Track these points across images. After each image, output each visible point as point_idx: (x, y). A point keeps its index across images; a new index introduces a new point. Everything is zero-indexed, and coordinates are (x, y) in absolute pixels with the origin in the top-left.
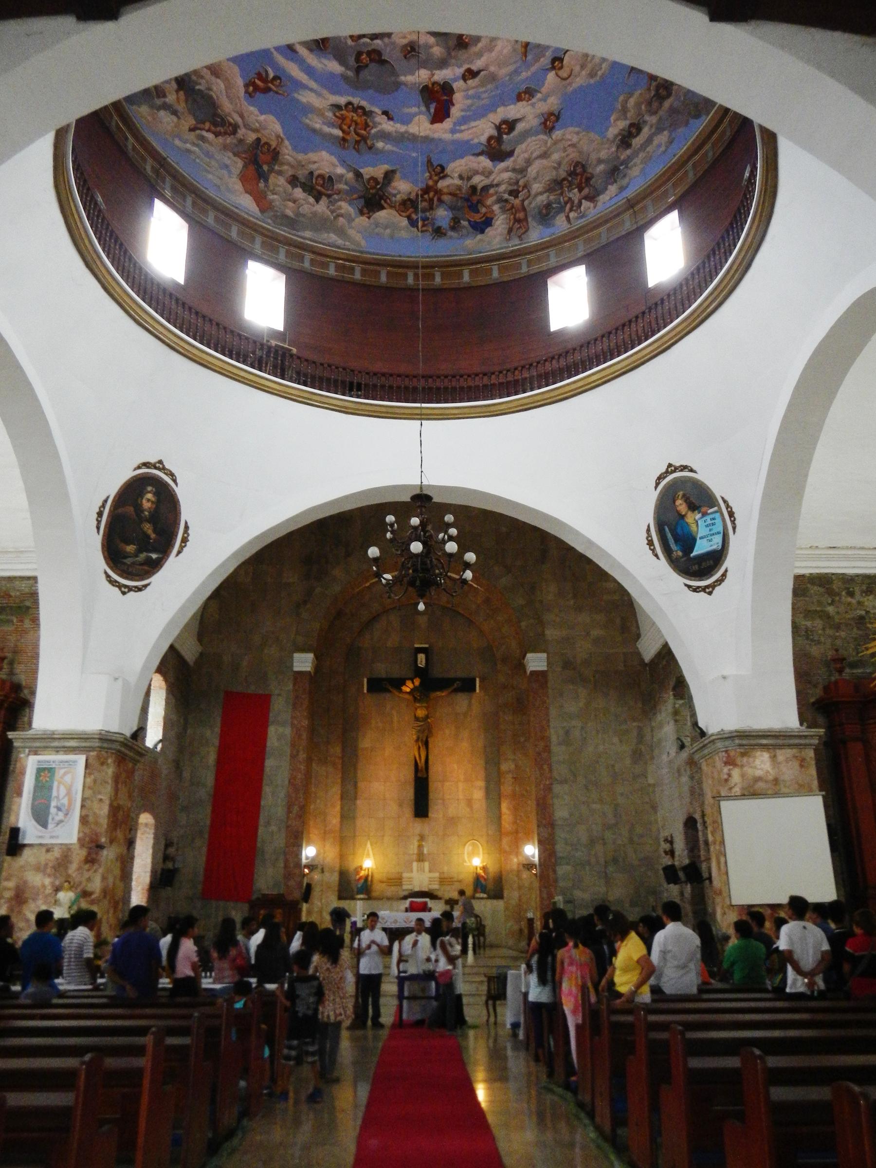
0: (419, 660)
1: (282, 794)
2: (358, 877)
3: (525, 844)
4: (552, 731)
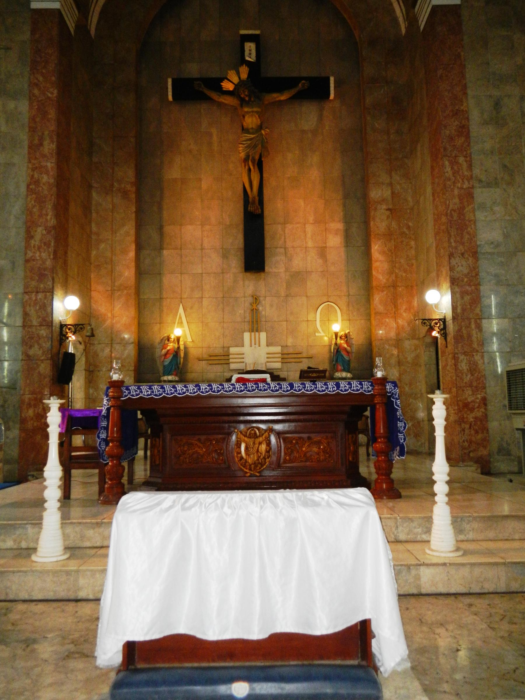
0: (247, 53)
1: (16, 208)
2: (164, 351)
3: (428, 287)
4: (471, 102)
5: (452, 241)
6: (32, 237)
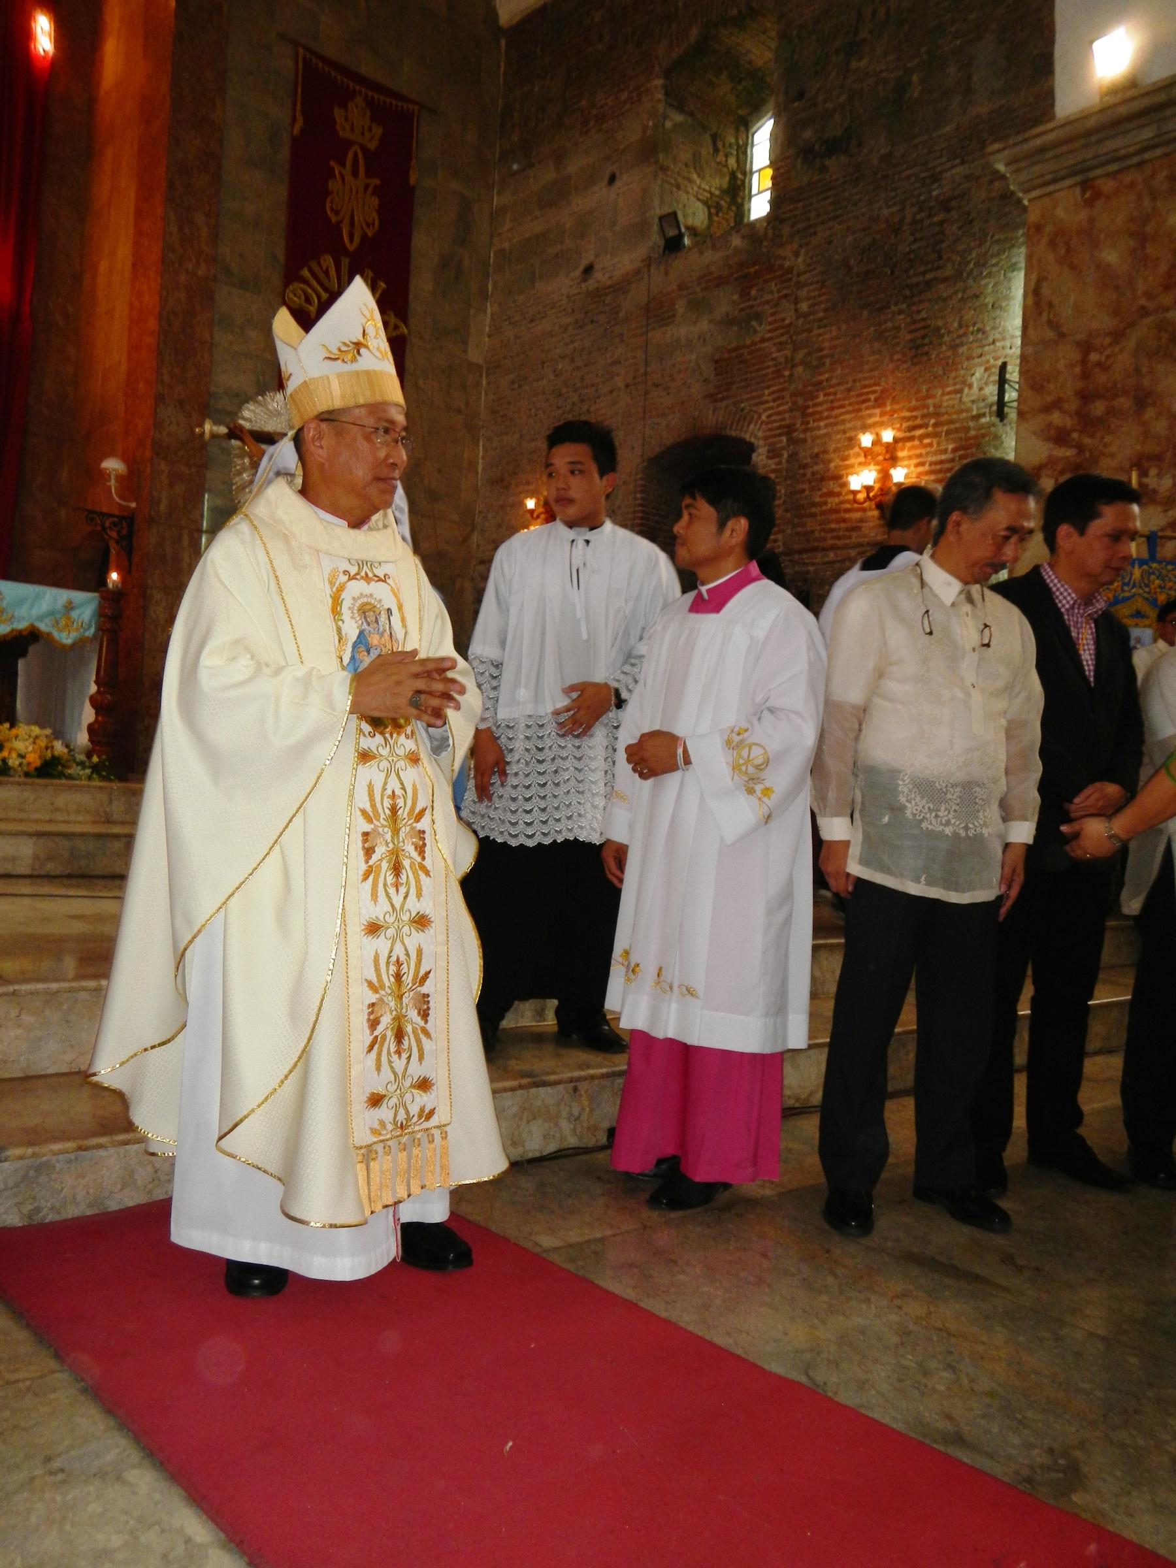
5: (165, 371)
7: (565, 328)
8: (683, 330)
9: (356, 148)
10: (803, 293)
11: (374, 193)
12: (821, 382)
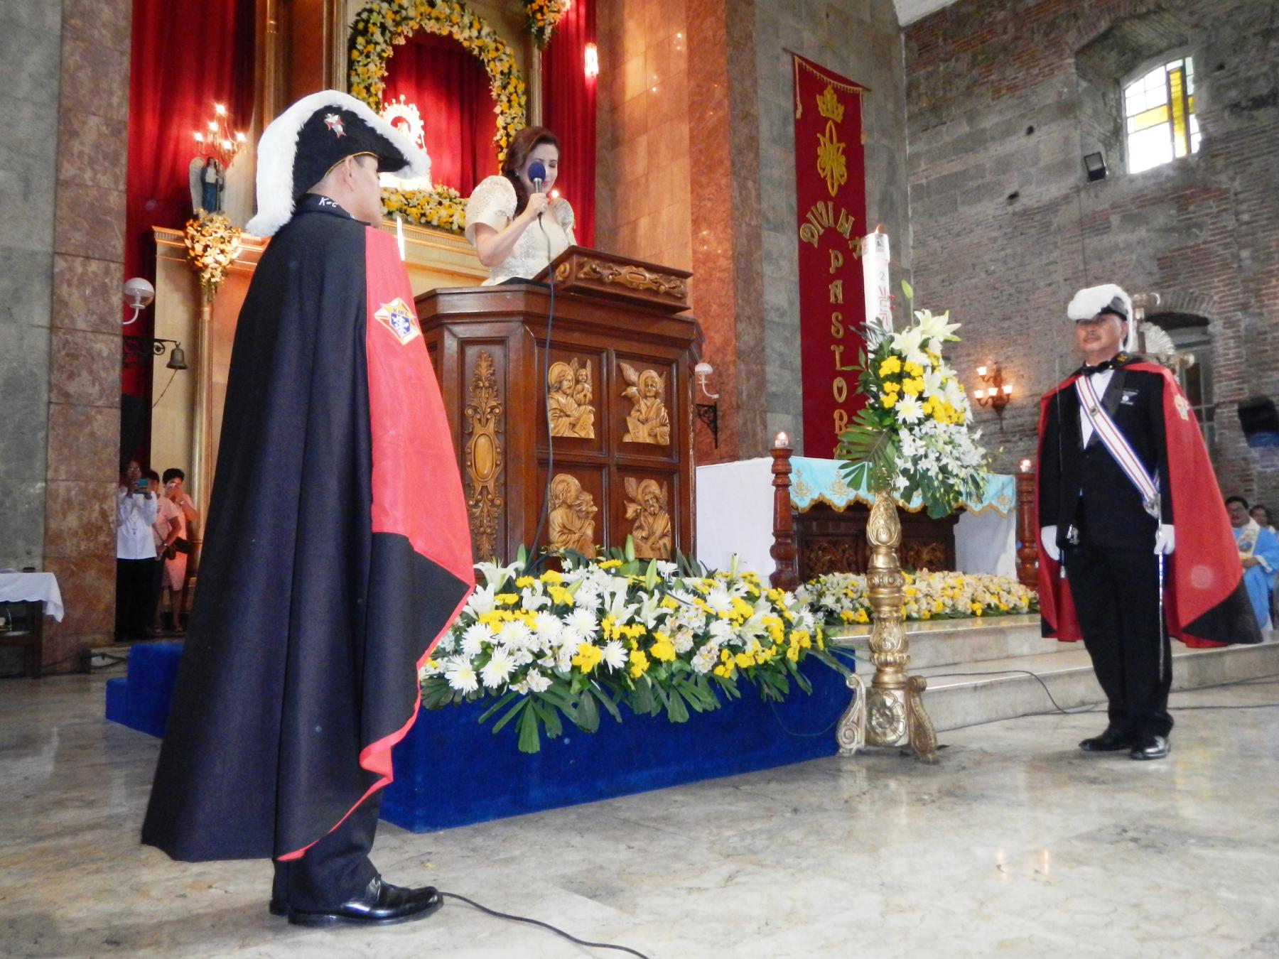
1: (36, 60)
6: (75, 134)
7: (995, 240)
8: (1121, 239)
9: (830, 123)
10: (1244, 207)
11: (843, 153)
12: (1271, 271)
